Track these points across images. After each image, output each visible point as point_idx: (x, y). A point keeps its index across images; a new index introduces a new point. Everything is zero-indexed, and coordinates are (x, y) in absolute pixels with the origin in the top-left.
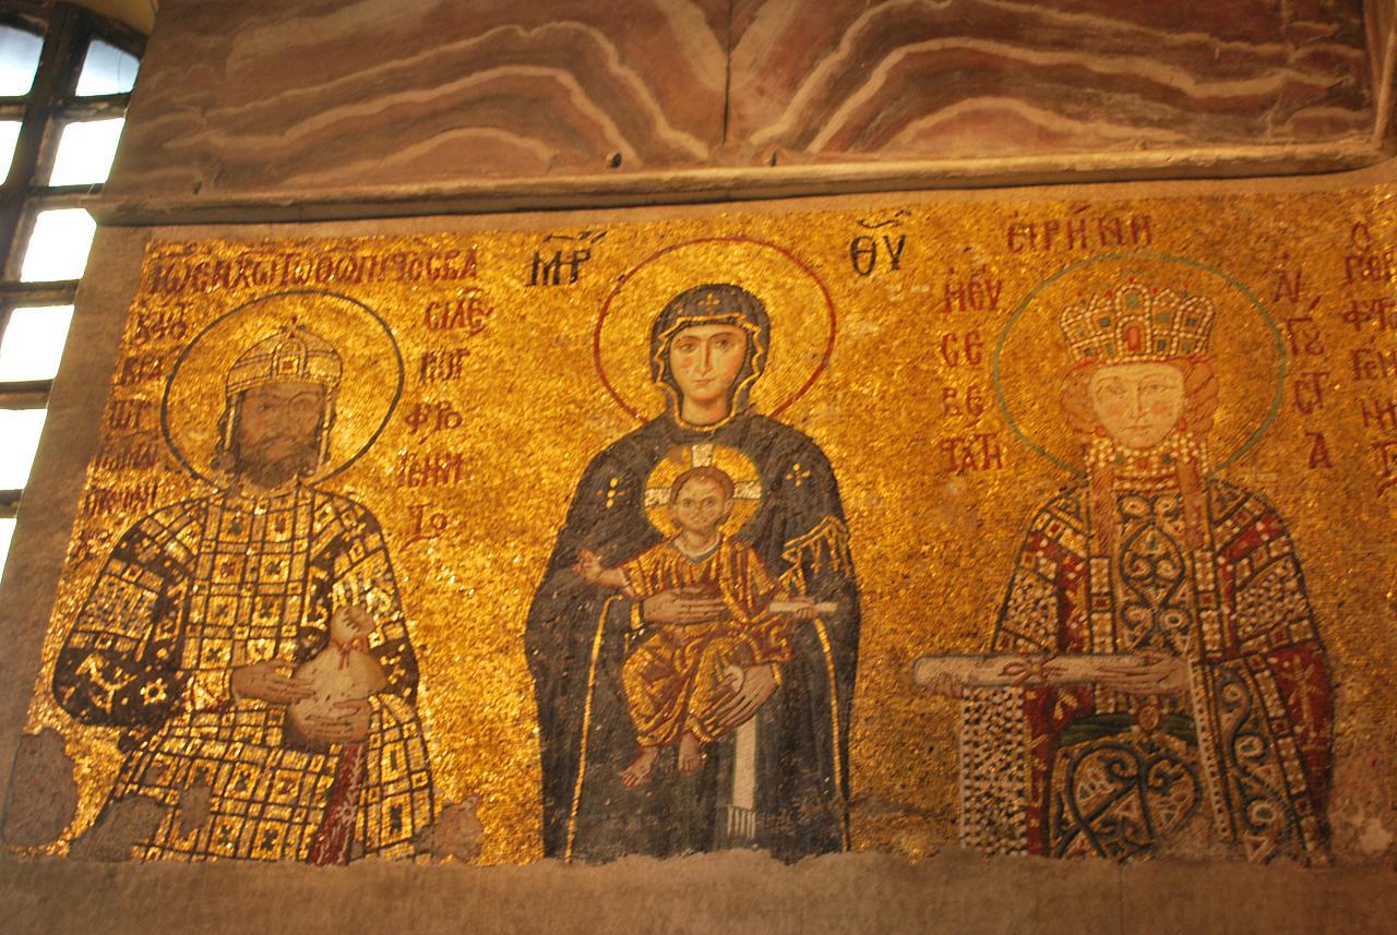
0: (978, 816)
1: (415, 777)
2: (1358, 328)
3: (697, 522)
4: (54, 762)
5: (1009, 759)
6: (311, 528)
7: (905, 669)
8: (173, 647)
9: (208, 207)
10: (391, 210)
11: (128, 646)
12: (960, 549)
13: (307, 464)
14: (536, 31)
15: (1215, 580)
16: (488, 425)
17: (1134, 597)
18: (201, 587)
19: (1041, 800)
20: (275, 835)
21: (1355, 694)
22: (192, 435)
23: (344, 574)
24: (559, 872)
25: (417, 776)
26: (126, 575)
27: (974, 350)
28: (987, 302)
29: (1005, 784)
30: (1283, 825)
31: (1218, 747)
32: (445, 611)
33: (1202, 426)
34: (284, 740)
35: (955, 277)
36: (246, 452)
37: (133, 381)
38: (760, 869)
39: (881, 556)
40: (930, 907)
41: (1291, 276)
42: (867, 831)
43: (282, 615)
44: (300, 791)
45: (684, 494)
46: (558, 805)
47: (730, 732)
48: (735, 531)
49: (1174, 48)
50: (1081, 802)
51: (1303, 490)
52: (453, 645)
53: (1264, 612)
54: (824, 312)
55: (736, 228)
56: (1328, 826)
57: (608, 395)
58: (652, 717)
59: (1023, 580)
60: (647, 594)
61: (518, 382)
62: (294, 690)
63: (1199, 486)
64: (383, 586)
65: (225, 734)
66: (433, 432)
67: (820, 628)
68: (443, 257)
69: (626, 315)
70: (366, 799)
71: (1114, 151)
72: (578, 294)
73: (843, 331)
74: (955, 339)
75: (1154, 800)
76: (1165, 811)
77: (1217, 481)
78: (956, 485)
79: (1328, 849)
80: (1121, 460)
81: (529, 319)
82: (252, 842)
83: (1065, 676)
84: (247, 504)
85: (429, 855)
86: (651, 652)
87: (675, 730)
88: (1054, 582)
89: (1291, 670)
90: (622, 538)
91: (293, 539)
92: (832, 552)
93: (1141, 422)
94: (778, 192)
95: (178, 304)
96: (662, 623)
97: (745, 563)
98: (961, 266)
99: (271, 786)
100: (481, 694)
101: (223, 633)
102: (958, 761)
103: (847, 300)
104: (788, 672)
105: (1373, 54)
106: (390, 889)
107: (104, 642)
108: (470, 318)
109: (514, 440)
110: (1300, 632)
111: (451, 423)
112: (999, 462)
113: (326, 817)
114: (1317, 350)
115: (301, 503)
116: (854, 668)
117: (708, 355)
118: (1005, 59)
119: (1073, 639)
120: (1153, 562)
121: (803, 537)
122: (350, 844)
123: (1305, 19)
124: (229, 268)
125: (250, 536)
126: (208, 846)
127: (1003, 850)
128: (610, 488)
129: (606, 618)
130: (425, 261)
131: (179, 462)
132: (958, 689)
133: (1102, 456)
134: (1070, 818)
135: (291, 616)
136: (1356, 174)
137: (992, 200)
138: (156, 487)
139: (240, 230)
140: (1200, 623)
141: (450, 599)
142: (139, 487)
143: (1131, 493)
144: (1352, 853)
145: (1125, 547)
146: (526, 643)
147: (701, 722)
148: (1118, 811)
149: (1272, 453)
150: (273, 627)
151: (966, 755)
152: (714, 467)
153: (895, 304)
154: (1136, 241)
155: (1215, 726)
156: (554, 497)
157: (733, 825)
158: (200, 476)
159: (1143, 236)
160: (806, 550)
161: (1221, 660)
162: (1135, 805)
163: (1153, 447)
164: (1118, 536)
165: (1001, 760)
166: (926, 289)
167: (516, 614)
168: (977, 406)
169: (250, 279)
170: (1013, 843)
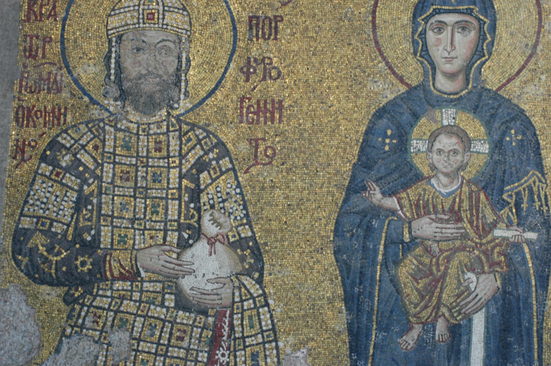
1: (265, 334)
4: (21, 309)
6: (181, 148)
8: (93, 232)
22: (86, 67)
25: (267, 333)
32: (278, 219)
43: (166, 214)
44: (191, 339)
45: (437, 145)
46: (359, 359)
54: (534, 10)
57: (384, 63)
58: (416, 305)
62: (180, 268)
66: (260, 81)
67: (526, 250)
84: (134, 127)
86: (416, 259)
90: (395, 176)
92: (536, 197)
96: (424, 239)
99: (171, 334)
100: (306, 280)
101: (125, 223)
104: (506, 280)
107: (43, 224)
111: (274, 73)
113: (209, 358)
115: (171, 129)
116: (548, 280)
121: (516, 184)
125: (138, 153)
129: (386, 233)
141: (282, 211)
142: (53, 109)
147: (450, 310)
156: (348, 140)
158: (98, 104)
167: (326, 225)
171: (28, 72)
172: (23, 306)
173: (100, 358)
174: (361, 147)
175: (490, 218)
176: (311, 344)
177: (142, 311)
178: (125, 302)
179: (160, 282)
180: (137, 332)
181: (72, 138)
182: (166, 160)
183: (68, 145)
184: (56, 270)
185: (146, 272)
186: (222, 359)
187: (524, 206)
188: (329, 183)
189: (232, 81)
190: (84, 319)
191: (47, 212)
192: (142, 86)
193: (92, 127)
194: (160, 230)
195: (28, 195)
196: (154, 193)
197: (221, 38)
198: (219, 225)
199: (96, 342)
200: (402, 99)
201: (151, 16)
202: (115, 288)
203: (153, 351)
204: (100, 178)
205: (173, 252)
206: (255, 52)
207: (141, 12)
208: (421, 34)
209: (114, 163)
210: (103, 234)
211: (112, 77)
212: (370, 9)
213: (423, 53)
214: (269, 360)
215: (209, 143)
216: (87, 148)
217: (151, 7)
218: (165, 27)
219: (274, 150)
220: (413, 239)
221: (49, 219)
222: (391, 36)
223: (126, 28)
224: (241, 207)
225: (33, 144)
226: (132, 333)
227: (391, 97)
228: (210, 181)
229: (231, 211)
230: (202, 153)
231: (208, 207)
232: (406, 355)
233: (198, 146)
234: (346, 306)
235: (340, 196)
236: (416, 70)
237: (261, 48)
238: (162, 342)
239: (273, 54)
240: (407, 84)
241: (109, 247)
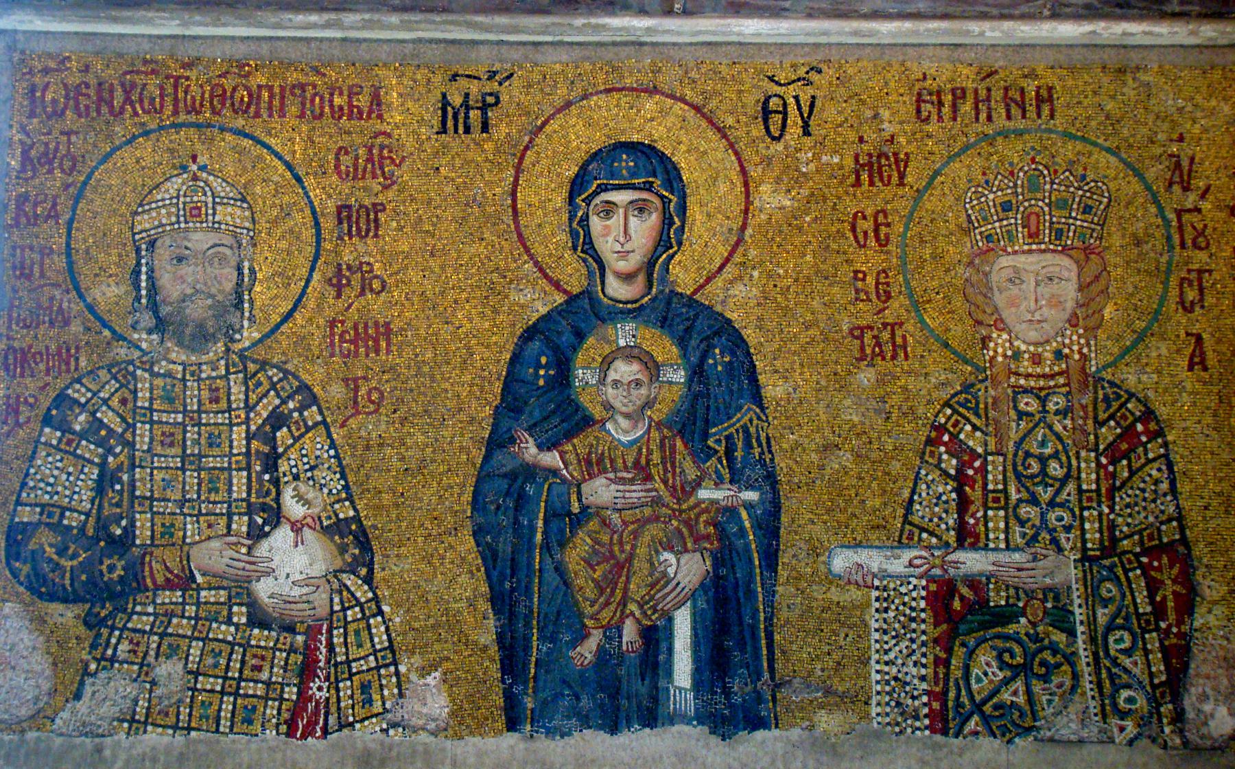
0: (887, 698)
1: (379, 655)
5: (914, 646)
7: (822, 559)
8: (124, 523)
13: (231, 327)
15: (1098, 481)
17: (1025, 495)
19: (941, 682)
21: (1214, 593)
22: (104, 288)
23: (288, 448)
24: (522, 746)
27: (883, 230)
28: (895, 179)
30: (1145, 710)
31: (1093, 640)
33: (1091, 323)
34: (249, 615)
35: (865, 147)
38: (700, 744)
39: (797, 445)
41: (1185, 163)
42: (793, 711)
43: (230, 491)
45: (612, 375)
50: (975, 686)
51: (1180, 393)
53: (1139, 513)
56: (1183, 710)
59: (926, 475)
61: (439, 246)
62: (253, 567)
63: (1087, 386)
66: (357, 297)
67: (744, 515)
68: (346, 93)
71: (1023, 17)
72: (488, 146)
73: (757, 203)
74: (864, 218)
75: (1037, 687)
77: (1103, 380)
78: (866, 377)
80: (1017, 355)
83: (963, 570)
85: (400, 730)
87: (618, 614)
88: (954, 478)
90: (556, 420)
93: (1037, 317)
95: (62, 133)
97: (673, 448)
98: (870, 136)
99: (243, 662)
102: (869, 648)
103: (759, 169)
106: (365, 759)
107: (50, 515)
108: (382, 168)
110: (1170, 533)
111: (376, 285)
113: (299, 694)
114: (1203, 245)
122: (326, 720)
125: (185, 406)
126: (190, 721)
127: (909, 730)
128: (538, 366)
129: (546, 502)
130: (327, 96)
132: (869, 579)
133: (1000, 350)
134: (967, 702)
137: (901, 58)
140: (1082, 519)
141: (395, 477)
143: (1026, 391)
144: (1202, 737)
145: (1018, 444)
147: (641, 606)
148: (1006, 696)
149: (1154, 354)
151: (877, 641)
154: (1039, 116)
155: (1091, 621)
157: (675, 704)
158: (125, 339)
159: (1046, 110)
160: (728, 438)
161: (1097, 558)
162: (1022, 689)
163: (1047, 341)
164: (1012, 434)
166: (836, 160)
167: (459, 495)
169: (137, 106)
170: (918, 724)
171: (20, 299)
172: (25, 635)
173: (141, 703)
174: (505, 382)
175: (692, 473)
176: (446, 665)
177: (200, 632)
178: (175, 621)
179: (224, 588)
180: (193, 662)
181: (89, 390)
182: (227, 415)
183: (83, 400)
184: (72, 579)
185: (203, 575)
186: (318, 694)
187: (739, 454)
189: (317, 299)
190: (115, 649)
191: (56, 497)
192: (188, 311)
193: (117, 372)
194: (223, 514)
195: (27, 475)
196: (210, 462)
198: (307, 503)
199: (135, 680)
200: (559, 313)
201: (195, 212)
202: (159, 601)
203: (218, 688)
204: (132, 445)
205: (243, 545)
206: (347, 257)
207: (181, 206)
208: (581, 220)
209: (152, 422)
210: (138, 524)
211: (144, 301)
212: (508, 188)
213: (586, 247)
214: (386, 692)
215: (288, 388)
216: (110, 403)
217: (195, 199)
218: (216, 226)
219: (382, 393)
220: (584, 509)
221: (59, 507)
222: (540, 225)
223: (160, 230)
224: (338, 476)
225: (31, 400)
226: (186, 664)
227: (543, 310)
228: (291, 441)
229: (323, 482)
230: (277, 402)
231: (290, 478)
232: (582, 674)
233: (272, 393)
234: (493, 609)
235: (478, 455)
236: (578, 270)
237: (356, 250)
238: (230, 674)
239: (374, 257)
240: (565, 292)
241: (148, 542)
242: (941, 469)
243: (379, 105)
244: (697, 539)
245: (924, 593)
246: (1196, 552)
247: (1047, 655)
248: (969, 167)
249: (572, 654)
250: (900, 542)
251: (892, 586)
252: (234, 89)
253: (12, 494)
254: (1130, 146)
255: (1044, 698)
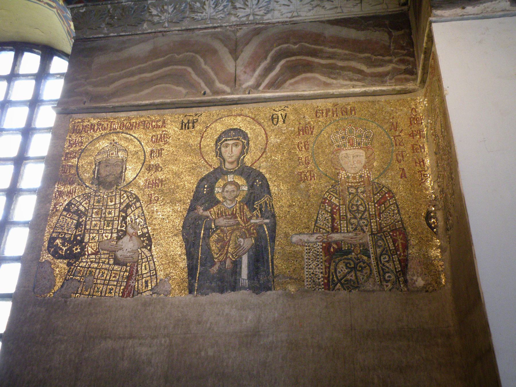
0: (310, 279)
2: (413, 138)
3: (230, 197)
5: (318, 263)
6: (120, 201)
8: (82, 236)
9: (87, 108)
10: (140, 108)
11: (69, 236)
12: (304, 204)
14: (181, 55)
15: (375, 211)
16: (170, 170)
17: (352, 216)
18: (89, 219)
20: (112, 289)
21: (414, 242)
22: (85, 174)
23: (130, 214)
24: (193, 298)
26: (67, 216)
27: (307, 146)
28: (310, 133)
29: (318, 270)
31: (376, 259)
34: (114, 262)
35: (301, 125)
36: (101, 179)
37: (68, 159)
39: (282, 206)
40: (297, 306)
41: (395, 124)
43: (112, 226)
44: (119, 277)
45: (226, 189)
46: (192, 279)
47: (240, 258)
48: (240, 200)
49: (361, 58)
50: (338, 275)
51: (399, 185)
52: (162, 234)
53: (388, 220)
54: (264, 136)
55: (239, 112)
56: (407, 280)
58: (217, 254)
60: (216, 218)
63: (370, 184)
64: (141, 217)
65: (97, 261)
67: (265, 227)
69: (208, 138)
70: (138, 279)
71: (345, 88)
72: (195, 132)
73: (270, 141)
75: (359, 274)
76: (362, 277)
78: (302, 185)
79: (407, 286)
80: (348, 177)
81: (181, 139)
82: (106, 291)
84: (102, 195)
88: (330, 213)
89: (396, 236)
91: (115, 204)
93: (354, 166)
94: (250, 101)
95: (80, 137)
96: (220, 226)
97: (244, 209)
98: (302, 122)
99: (111, 275)
100: (170, 248)
101: (96, 232)
104: (256, 240)
105: (417, 59)
106: (145, 304)
107: (62, 235)
108: (164, 140)
109: (177, 175)
110: (399, 225)
111: (159, 170)
112: (314, 178)
113: (126, 284)
116: (275, 238)
117: (232, 149)
118: (313, 62)
119: (336, 229)
120: (358, 206)
123: (398, 49)
124: (94, 126)
126: (93, 293)
127: (317, 289)
128: (205, 188)
130: (151, 123)
131: (82, 182)
132: (304, 244)
133: (343, 176)
134: (336, 279)
135: (115, 227)
136: (412, 94)
138: (75, 190)
139: (98, 115)
140: (371, 223)
142: (70, 190)
143: (351, 187)
145: (350, 202)
146: (182, 233)
148: (349, 277)
150: (110, 230)
151: (306, 262)
152: (235, 181)
153: (284, 133)
159: (353, 112)
160: (260, 205)
161: (377, 234)
162: (354, 275)
163: (357, 173)
165: (316, 263)
166: (293, 129)
167: (179, 225)
168: (308, 162)
170: (320, 287)
179: (107, 254)
184: (65, 252)
185: (102, 250)
186: (132, 284)
188: (181, 208)
197: (139, 158)
208: (219, 148)
211: (95, 178)
219: (158, 197)
227: (207, 173)
235: (185, 214)
236: (217, 162)
240: (213, 168)
242: (326, 210)
243: (165, 123)
244: (251, 234)
245: (321, 247)
246: (407, 231)
247: (361, 264)
248: (332, 128)
249: (210, 270)
250: (313, 232)
251: (311, 245)
252: (127, 123)
253: (52, 229)
254: (378, 120)
255: (361, 277)
